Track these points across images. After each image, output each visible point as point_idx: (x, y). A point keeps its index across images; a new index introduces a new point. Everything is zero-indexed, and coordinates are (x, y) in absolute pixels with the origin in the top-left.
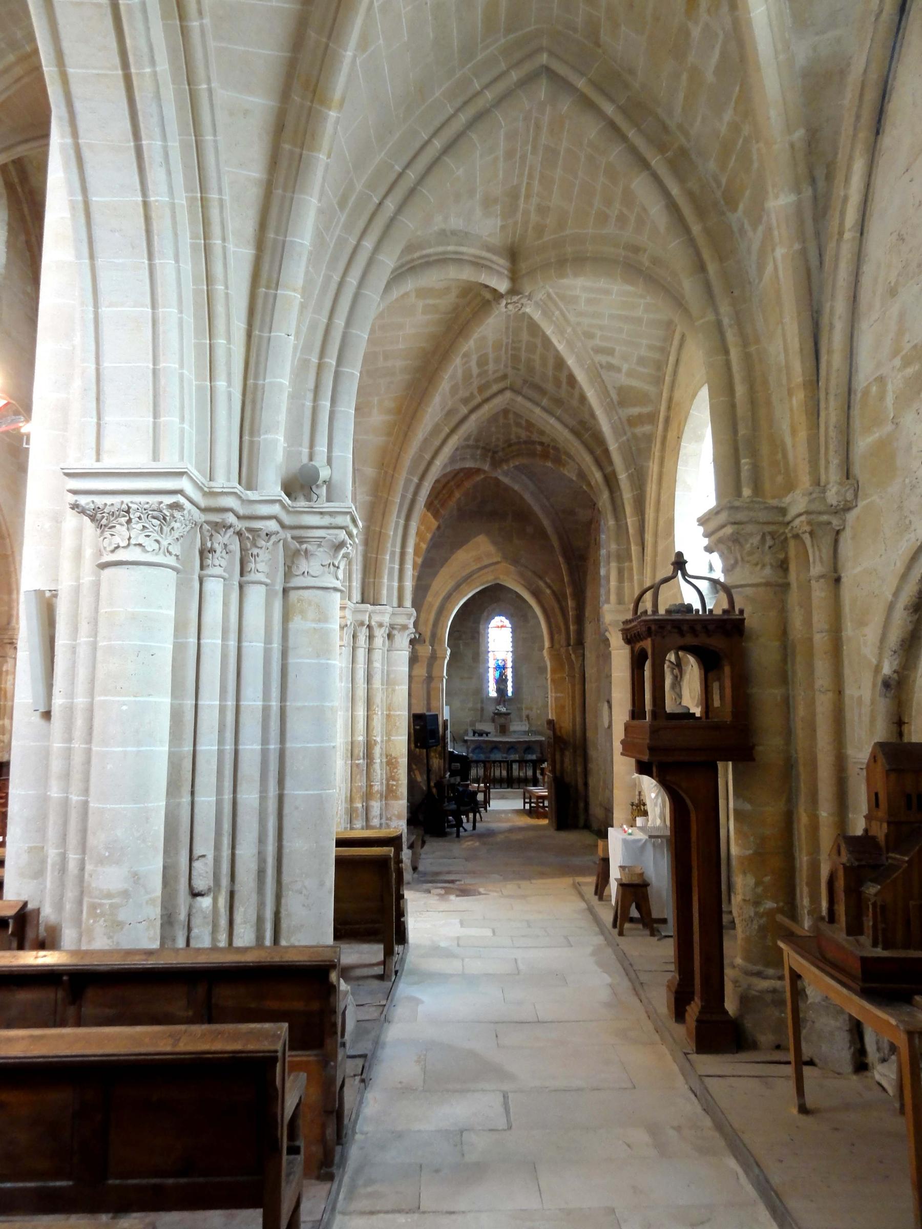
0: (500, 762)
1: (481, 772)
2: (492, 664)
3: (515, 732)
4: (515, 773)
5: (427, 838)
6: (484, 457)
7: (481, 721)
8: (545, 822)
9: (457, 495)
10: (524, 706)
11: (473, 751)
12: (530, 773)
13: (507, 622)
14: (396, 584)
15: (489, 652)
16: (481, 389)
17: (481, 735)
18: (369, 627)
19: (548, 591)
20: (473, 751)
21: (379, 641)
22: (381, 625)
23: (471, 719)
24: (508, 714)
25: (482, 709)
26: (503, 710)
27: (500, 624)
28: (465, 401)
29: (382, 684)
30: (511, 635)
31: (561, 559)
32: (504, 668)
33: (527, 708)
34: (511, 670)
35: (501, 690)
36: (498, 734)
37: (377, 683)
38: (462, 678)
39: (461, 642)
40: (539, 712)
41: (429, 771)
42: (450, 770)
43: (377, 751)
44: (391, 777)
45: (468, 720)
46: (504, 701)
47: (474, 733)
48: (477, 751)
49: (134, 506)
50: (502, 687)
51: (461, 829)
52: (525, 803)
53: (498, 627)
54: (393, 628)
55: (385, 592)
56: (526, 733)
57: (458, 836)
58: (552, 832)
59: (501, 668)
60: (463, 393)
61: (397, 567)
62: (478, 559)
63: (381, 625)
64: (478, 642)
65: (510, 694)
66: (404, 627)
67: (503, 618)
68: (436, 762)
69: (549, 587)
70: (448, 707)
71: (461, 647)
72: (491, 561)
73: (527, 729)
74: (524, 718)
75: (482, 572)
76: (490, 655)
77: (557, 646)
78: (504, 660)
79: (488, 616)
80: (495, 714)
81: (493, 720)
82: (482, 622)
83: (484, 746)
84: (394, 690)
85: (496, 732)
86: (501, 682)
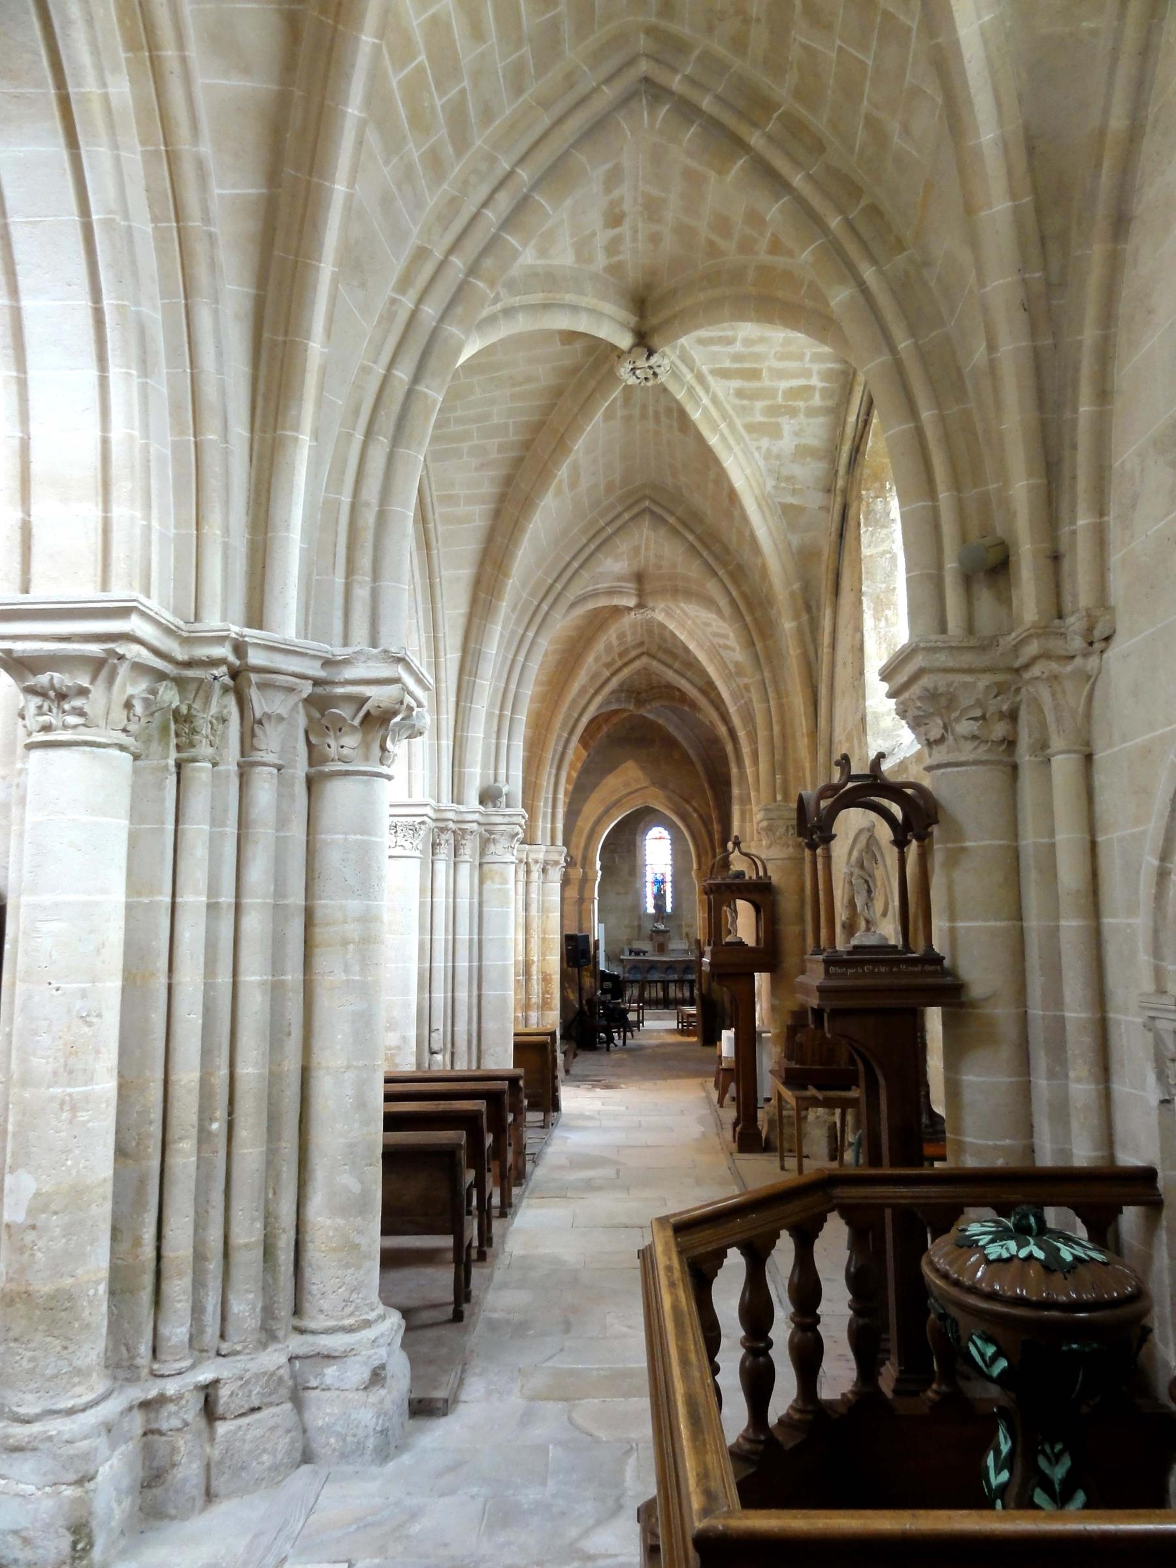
0: (656, 982)
1: (636, 992)
2: (650, 878)
4: (672, 994)
5: (578, 1052)
6: (628, 700)
8: (695, 1039)
9: (605, 729)
11: (629, 972)
12: (687, 994)
13: (665, 834)
14: (549, 826)
16: (621, 655)
17: (637, 954)
18: (526, 863)
19: (695, 815)
21: (536, 874)
22: (536, 862)
24: (667, 932)
25: (639, 927)
26: (662, 927)
28: (608, 665)
29: (538, 912)
31: (706, 786)
32: (663, 882)
35: (660, 907)
37: (534, 911)
39: (616, 855)
41: (581, 989)
42: (602, 989)
43: (534, 969)
44: (546, 991)
46: (663, 918)
47: (631, 952)
49: (399, 824)
50: (660, 903)
51: (612, 1045)
52: (678, 1023)
54: (547, 864)
55: (540, 833)
57: (608, 1049)
58: (699, 1048)
59: (659, 883)
60: (606, 659)
61: (550, 810)
62: (626, 784)
63: (536, 862)
64: (635, 856)
65: (669, 909)
66: (556, 863)
67: (661, 829)
68: (588, 981)
69: (696, 810)
70: (602, 926)
71: (617, 860)
72: (639, 786)
75: (629, 798)
76: (647, 868)
77: (704, 867)
81: (651, 938)
82: (639, 831)
84: (547, 917)
85: (654, 951)
86: (659, 897)
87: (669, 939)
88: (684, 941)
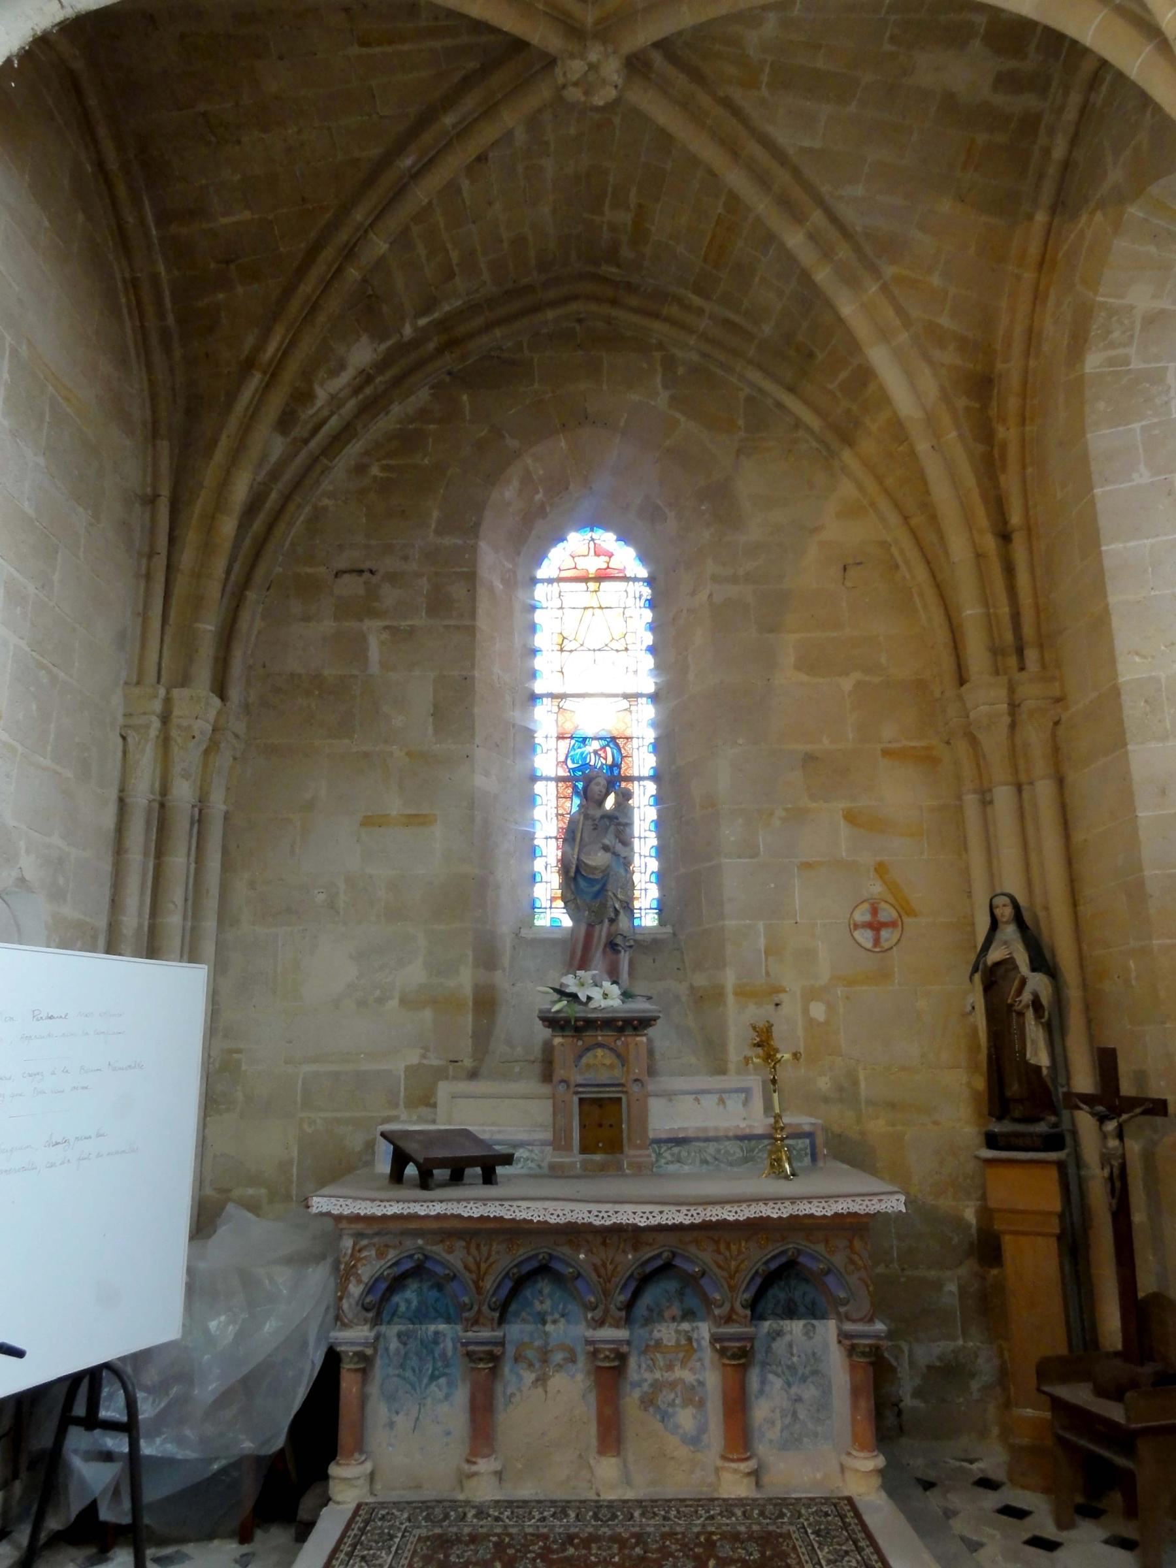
7: (473, 1075)
10: (730, 979)
13: (626, 558)
15: (534, 698)
24: (639, 1024)
27: (593, 565)
30: (648, 615)
33: (743, 993)
34: (651, 788)
36: (575, 1158)
40: (818, 1011)
45: (398, 1066)
46: (612, 946)
48: (407, 1298)
50: (599, 859)
53: (585, 579)
65: (646, 917)
67: (607, 539)
73: (759, 1123)
74: (737, 1044)
80: (553, 1022)
83: (456, 1257)
85: (559, 1142)
87: (651, 1071)
88: (731, 1081)
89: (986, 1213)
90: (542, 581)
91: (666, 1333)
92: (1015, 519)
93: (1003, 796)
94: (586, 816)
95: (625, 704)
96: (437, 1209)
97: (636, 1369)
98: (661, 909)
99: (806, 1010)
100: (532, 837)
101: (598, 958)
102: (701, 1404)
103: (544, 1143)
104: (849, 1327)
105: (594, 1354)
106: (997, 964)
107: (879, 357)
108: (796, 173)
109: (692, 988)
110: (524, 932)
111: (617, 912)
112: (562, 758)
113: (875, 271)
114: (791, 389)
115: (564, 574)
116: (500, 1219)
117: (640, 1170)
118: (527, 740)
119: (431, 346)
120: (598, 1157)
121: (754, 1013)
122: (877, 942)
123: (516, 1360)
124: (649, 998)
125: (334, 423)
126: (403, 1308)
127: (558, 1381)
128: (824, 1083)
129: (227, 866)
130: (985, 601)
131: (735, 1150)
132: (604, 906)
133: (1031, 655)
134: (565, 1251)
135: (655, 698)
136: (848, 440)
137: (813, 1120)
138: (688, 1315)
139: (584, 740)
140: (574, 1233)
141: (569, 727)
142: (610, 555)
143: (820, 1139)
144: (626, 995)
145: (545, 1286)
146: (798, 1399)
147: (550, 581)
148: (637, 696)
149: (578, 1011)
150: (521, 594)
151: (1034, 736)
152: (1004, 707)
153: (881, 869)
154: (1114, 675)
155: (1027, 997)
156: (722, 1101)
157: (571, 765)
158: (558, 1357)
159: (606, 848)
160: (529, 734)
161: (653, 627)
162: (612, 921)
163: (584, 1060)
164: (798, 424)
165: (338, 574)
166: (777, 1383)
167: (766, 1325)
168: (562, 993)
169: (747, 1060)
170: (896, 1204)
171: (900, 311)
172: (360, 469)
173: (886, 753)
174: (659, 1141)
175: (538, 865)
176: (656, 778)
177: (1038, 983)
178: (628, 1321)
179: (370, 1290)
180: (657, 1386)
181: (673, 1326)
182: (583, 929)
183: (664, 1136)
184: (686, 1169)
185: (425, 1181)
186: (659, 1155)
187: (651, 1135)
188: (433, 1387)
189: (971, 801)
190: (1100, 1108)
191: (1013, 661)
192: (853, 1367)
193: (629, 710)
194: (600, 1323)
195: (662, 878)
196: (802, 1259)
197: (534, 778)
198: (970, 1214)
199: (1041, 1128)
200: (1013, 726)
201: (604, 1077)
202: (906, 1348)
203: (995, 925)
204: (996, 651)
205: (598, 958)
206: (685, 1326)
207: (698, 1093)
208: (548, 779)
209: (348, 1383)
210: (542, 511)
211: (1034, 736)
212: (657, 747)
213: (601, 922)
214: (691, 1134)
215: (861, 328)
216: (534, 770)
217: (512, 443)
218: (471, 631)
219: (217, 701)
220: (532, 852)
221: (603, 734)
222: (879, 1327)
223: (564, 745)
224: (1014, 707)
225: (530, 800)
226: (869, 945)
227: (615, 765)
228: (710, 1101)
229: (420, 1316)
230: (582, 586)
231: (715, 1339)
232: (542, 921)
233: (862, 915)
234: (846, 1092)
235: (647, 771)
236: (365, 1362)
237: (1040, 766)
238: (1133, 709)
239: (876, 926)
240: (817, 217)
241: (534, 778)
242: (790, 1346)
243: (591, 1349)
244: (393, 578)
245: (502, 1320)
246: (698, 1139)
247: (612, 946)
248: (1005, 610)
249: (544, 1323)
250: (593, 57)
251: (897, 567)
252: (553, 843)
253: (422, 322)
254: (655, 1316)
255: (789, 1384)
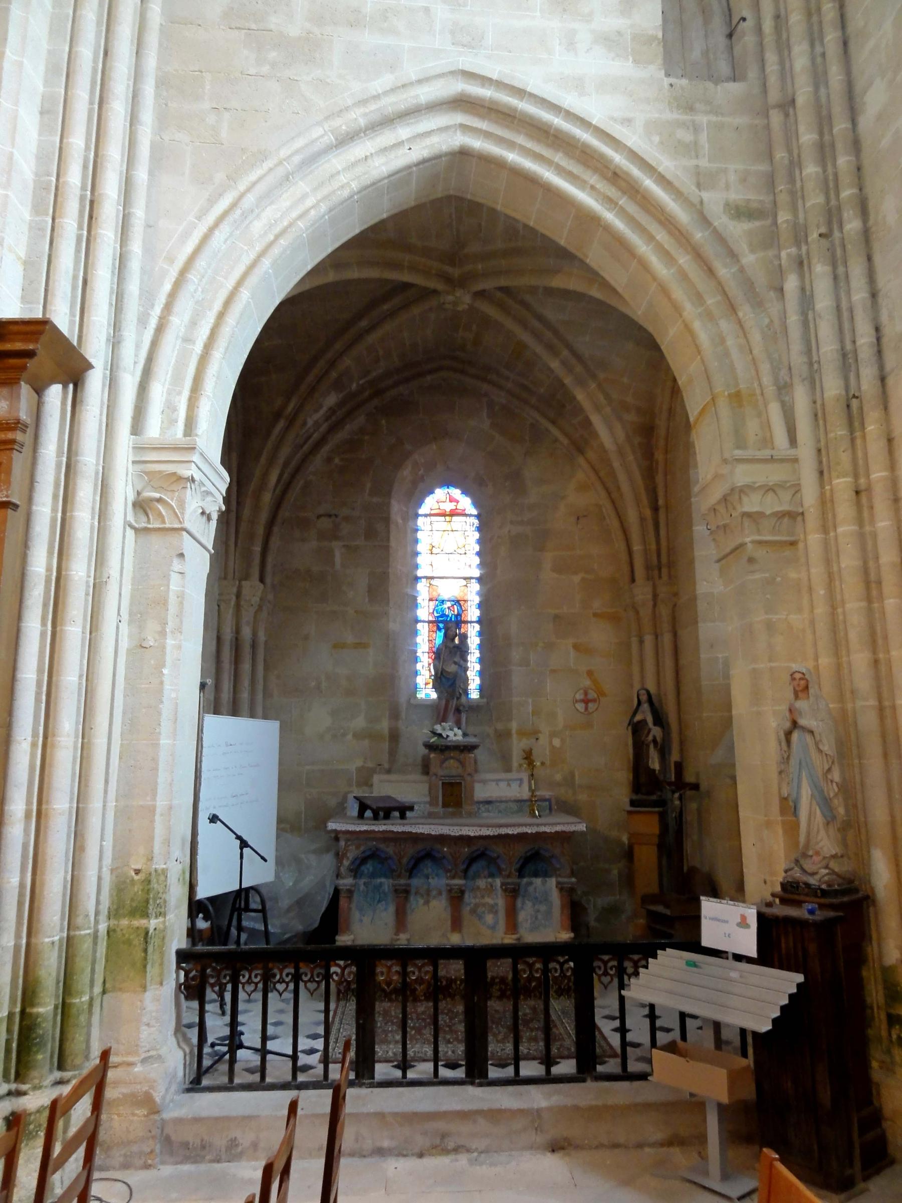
2: (424, 612)
3: (489, 802)
7: (389, 771)
10: (514, 726)
11: (355, 871)
13: (466, 503)
15: (417, 579)
20: (355, 871)
23: (359, 763)
24: (470, 748)
25: (394, 737)
26: (455, 735)
27: (448, 507)
32: (459, 621)
33: (522, 733)
34: (477, 627)
36: (439, 809)
38: (339, 646)
39: (337, 546)
40: (557, 742)
46: (458, 711)
47: (363, 807)
48: (368, 867)
50: (452, 668)
53: (443, 515)
56: (529, 805)
65: (474, 695)
67: (456, 493)
71: (338, 559)
73: (525, 794)
74: (516, 758)
76: (422, 586)
78: (457, 602)
79: (415, 484)
80: (430, 747)
81: (426, 768)
83: (390, 850)
87: (476, 771)
88: (514, 775)
89: (632, 836)
90: (422, 515)
91: (482, 883)
92: (661, 502)
93: (649, 639)
94: (446, 647)
95: (464, 582)
96: (382, 828)
97: (469, 899)
98: (481, 689)
99: (551, 743)
100: (416, 652)
101: (451, 716)
102: (496, 913)
103: (425, 803)
104: (560, 879)
105: (450, 891)
106: (639, 722)
107: (596, 420)
108: (556, 332)
109: (496, 730)
110: (412, 701)
111: (460, 694)
112: (431, 611)
113: (594, 376)
114: (553, 422)
115: (433, 512)
116: (411, 833)
117: (470, 815)
118: (413, 603)
119: (367, 394)
120: (450, 810)
121: (525, 743)
122: (586, 709)
123: (416, 894)
124: (475, 736)
125: (316, 436)
126: (366, 871)
127: (434, 903)
128: (558, 777)
129: (267, 668)
130: (644, 542)
131: (514, 806)
132: (454, 691)
133: (664, 571)
134: (438, 846)
135: (480, 580)
136: (581, 451)
137: (550, 794)
138: (492, 875)
139: (443, 602)
140: (443, 839)
141: (435, 594)
142: (457, 502)
143: (553, 802)
144: (465, 735)
145: (429, 863)
146: (538, 911)
147: (426, 516)
148: (471, 578)
149: (442, 742)
150: (411, 524)
151: (664, 611)
152: (650, 597)
153: (590, 673)
154: (694, 590)
155: (650, 738)
156: (509, 785)
157: (436, 615)
158: (434, 893)
159: (455, 663)
160: (415, 599)
161: (479, 542)
162: (458, 699)
163: (444, 765)
164: (556, 440)
165: (319, 517)
166: (529, 904)
167: (525, 880)
168: (434, 733)
169: (521, 765)
170: (582, 827)
171: (607, 397)
172: (329, 460)
173: (595, 615)
174: (479, 802)
175: (419, 666)
176: (479, 622)
177: (656, 732)
178: (465, 877)
179: (353, 863)
180: (477, 906)
181: (484, 880)
182: (444, 702)
183: (481, 800)
184: (491, 814)
185: (376, 817)
186: (479, 809)
187: (476, 799)
188: (380, 905)
189: (635, 641)
190: (674, 787)
191: (656, 572)
192: (562, 897)
193: (466, 586)
194: (453, 877)
195: (481, 673)
196: (542, 852)
197: (417, 621)
198: (625, 839)
199: (654, 797)
200: (655, 605)
201: (454, 772)
202: (592, 900)
203: (639, 703)
204: (648, 568)
205: (451, 716)
206: (490, 880)
207: (497, 781)
208: (424, 622)
209: (343, 902)
210: (422, 479)
211: (664, 611)
212: (480, 606)
213: (453, 699)
214: (494, 799)
215: (587, 405)
216: (417, 616)
217: (408, 447)
218: (387, 548)
219: (262, 586)
220: (416, 660)
221: (453, 598)
222: (574, 880)
223: (432, 604)
224: (655, 596)
225: (415, 633)
226: (582, 710)
227: (459, 615)
228: (503, 785)
229: (373, 875)
230: (442, 518)
231: (502, 884)
232: (421, 695)
233: (579, 696)
234: (569, 781)
235: (475, 619)
236: (350, 892)
237: (666, 626)
238: (701, 606)
239: (586, 702)
240: (565, 353)
241: (417, 621)
242: (535, 888)
243: (449, 888)
244: (347, 519)
245: (410, 877)
246: (497, 801)
247: (458, 711)
248: (653, 547)
249: (428, 878)
250: (458, 294)
251: (604, 518)
252: (426, 655)
253: (361, 382)
254: (477, 876)
255: (534, 905)
